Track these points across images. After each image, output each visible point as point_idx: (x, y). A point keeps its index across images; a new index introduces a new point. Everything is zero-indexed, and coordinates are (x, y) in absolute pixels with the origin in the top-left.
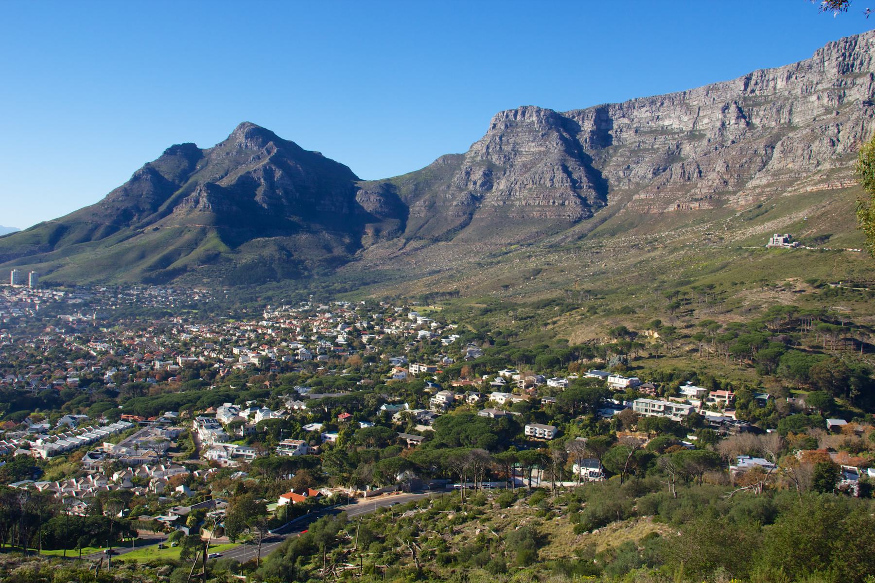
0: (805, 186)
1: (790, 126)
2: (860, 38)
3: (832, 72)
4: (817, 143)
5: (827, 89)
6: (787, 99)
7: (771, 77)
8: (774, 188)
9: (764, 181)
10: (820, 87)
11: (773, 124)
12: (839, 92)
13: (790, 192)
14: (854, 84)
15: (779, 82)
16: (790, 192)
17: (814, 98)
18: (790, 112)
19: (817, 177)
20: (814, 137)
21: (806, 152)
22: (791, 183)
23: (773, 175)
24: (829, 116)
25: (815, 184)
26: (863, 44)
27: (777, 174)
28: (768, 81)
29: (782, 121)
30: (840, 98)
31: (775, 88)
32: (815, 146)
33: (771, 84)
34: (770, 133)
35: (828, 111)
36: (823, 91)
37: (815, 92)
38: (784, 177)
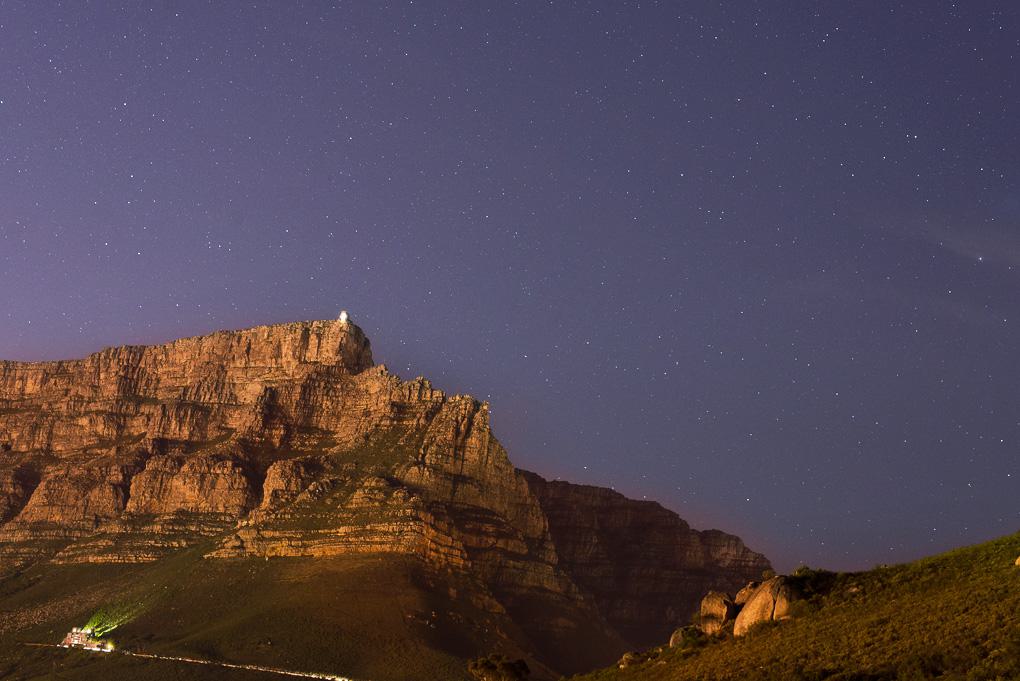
0: (83, 554)
1: (49, 456)
2: (147, 352)
3: (110, 390)
4: (96, 491)
5: (102, 412)
6: (45, 415)
7: (19, 374)
8: (36, 550)
9: (19, 537)
10: (93, 407)
11: (23, 448)
12: (116, 418)
13: (61, 559)
14: (137, 412)
15: (30, 382)
16: (61, 559)
17: (84, 421)
18: (50, 435)
19: (102, 543)
20: (87, 484)
21: (80, 503)
22: (60, 544)
23: (32, 529)
24: (104, 451)
25: (101, 553)
26: (150, 360)
27: (38, 526)
28: (14, 380)
29: (37, 446)
30: (120, 428)
31: (22, 390)
32: (94, 494)
33: (18, 384)
34: (19, 460)
35: (103, 442)
36: (98, 413)
37: (87, 413)
38: (49, 535)
